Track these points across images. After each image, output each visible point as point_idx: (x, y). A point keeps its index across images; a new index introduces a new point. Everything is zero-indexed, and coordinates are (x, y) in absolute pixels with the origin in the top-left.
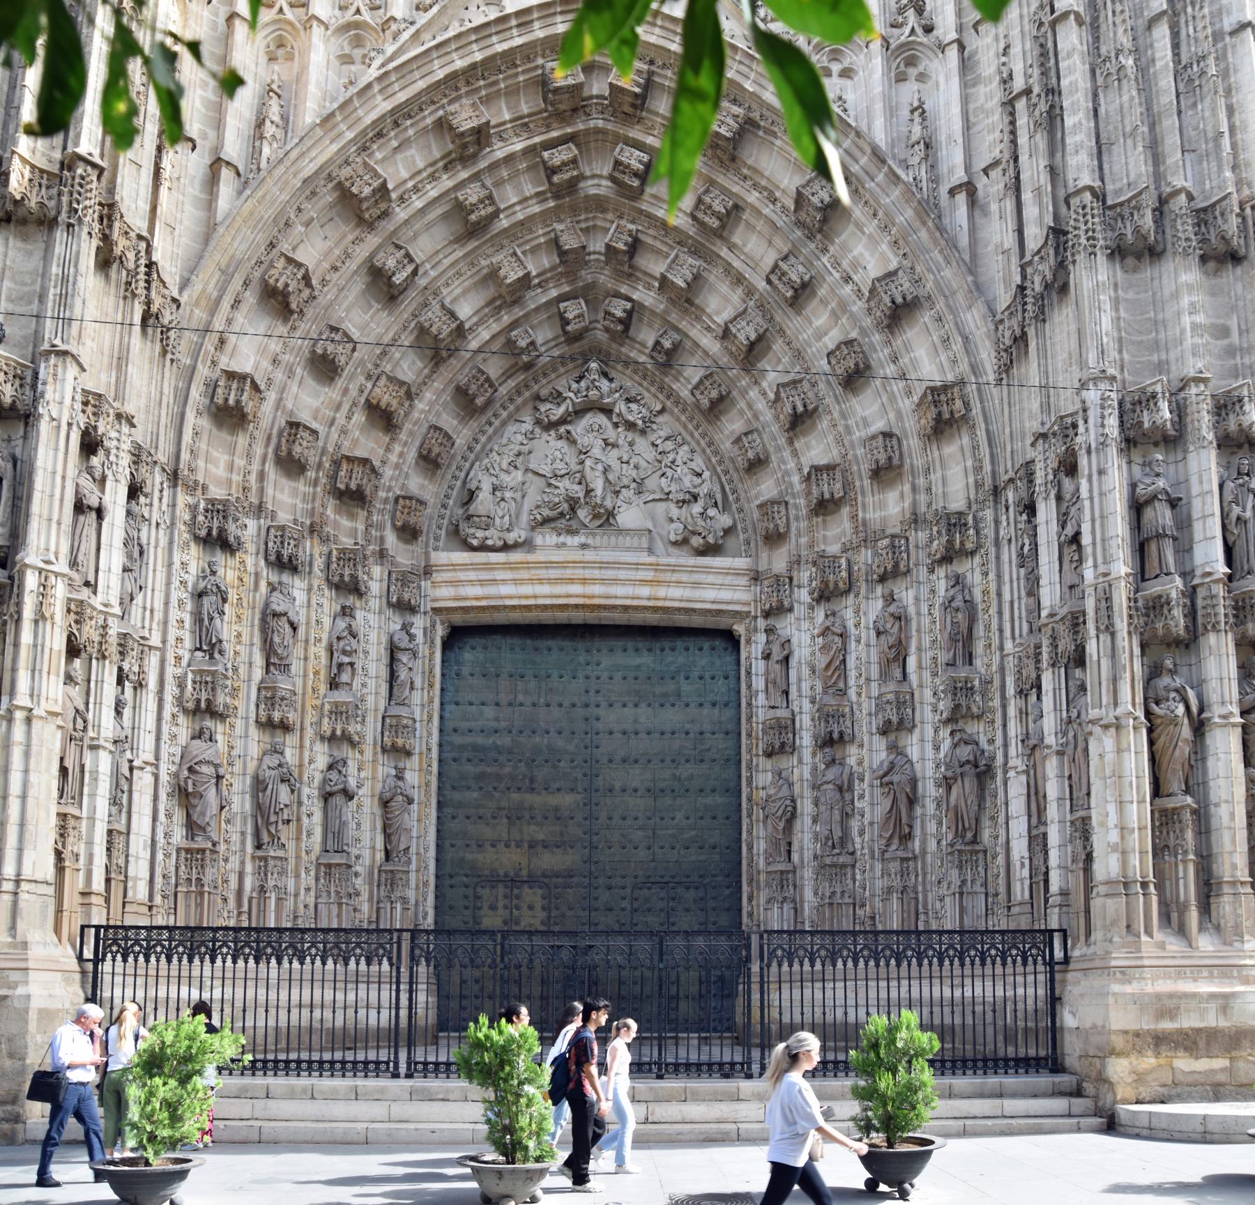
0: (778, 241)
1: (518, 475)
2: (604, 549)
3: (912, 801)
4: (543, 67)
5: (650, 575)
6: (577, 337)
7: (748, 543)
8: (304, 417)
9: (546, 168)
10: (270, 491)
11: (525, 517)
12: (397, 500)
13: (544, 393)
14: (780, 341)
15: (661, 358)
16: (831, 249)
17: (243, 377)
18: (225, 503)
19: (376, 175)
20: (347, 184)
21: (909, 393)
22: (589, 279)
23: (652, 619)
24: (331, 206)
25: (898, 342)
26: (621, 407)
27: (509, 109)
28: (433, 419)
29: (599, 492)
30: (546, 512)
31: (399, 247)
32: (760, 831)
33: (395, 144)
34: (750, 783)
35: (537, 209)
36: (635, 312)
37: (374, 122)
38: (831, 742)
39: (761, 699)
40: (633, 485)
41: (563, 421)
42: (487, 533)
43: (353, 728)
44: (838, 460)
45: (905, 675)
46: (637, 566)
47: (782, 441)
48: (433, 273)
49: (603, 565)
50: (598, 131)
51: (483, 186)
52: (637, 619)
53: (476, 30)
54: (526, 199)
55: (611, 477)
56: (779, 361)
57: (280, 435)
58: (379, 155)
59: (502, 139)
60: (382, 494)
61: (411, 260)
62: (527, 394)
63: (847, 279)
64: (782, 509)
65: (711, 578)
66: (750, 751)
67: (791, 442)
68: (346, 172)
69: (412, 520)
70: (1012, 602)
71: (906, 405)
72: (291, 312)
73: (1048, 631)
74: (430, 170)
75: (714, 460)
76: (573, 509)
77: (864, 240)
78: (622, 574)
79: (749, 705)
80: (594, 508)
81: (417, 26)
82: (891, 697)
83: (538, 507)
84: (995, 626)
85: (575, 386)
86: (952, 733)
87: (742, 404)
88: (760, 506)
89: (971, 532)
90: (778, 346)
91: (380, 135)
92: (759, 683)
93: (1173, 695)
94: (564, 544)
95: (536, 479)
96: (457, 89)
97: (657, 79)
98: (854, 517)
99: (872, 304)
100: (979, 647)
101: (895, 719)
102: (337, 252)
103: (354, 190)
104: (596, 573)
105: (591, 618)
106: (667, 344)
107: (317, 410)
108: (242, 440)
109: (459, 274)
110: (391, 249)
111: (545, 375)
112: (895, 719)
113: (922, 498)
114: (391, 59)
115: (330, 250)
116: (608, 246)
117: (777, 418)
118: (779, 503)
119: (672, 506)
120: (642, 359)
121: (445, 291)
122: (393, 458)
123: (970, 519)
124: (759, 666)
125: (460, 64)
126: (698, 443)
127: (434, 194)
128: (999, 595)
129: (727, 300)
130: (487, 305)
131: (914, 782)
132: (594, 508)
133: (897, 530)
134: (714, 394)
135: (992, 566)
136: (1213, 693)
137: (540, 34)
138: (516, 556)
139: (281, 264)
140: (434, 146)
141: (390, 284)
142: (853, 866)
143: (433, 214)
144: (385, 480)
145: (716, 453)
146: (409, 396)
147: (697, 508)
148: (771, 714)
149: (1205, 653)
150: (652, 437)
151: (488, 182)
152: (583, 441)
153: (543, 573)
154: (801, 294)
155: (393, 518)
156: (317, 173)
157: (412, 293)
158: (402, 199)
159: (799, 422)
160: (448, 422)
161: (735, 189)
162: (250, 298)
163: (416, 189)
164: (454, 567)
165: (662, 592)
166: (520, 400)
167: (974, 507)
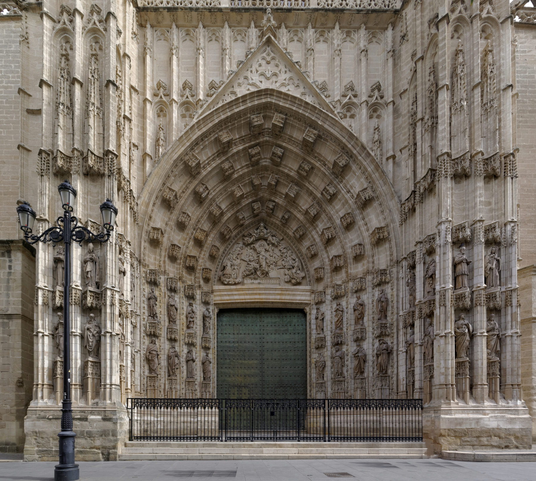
0: (326, 180)
1: (238, 261)
2: (265, 284)
3: (365, 361)
4: (250, 117)
5: (280, 292)
6: (257, 215)
7: (310, 281)
8: (176, 243)
9: (249, 155)
10: (167, 267)
11: (241, 274)
12: (203, 269)
13: (246, 234)
14: (324, 214)
15: (284, 222)
16: (344, 181)
17: (158, 229)
18: (155, 270)
19: (197, 159)
20: (187, 162)
21: (368, 230)
22: (262, 195)
23: (280, 306)
24: (182, 170)
25: (365, 213)
26: (270, 238)
27: (238, 134)
28: (213, 244)
29: (264, 266)
30: (248, 273)
31: (203, 184)
32: (313, 371)
33: (202, 147)
34: (310, 357)
35: (246, 170)
36: (277, 205)
37: (196, 139)
38: (338, 344)
39: (314, 332)
40: (274, 264)
41: (252, 243)
42: (230, 280)
43: (194, 341)
44: (342, 254)
45: (363, 323)
46: (276, 289)
47: (323, 248)
48: (214, 194)
49: (265, 289)
50: (267, 141)
51: (230, 162)
52: (275, 306)
53: (228, 103)
54: (243, 167)
55: (267, 261)
56: (323, 221)
57: (169, 249)
58: (197, 152)
59: (236, 145)
60: (199, 268)
61: (208, 189)
62: (241, 235)
63: (349, 192)
64: (322, 270)
65: (298, 293)
66: (310, 347)
67: (326, 248)
68: (187, 158)
69: (208, 276)
70: (403, 298)
71: (366, 234)
72: (171, 207)
73: (419, 307)
74: (213, 157)
75: (299, 255)
76: (255, 272)
77: (356, 177)
78: (271, 292)
79: (310, 333)
80: (262, 271)
81: (209, 102)
82: (359, 330)
83: (245, 271)
84: (395, 307)
85: (256, 231)
86: (379, 341)
87: (310, 236)
88: (315, 269)
89: (388, 276)
90: (323, 216)
91: (197, 144)
92: (313, 327)
93: (464, 326)
94: (253, 283)
95: (244, 262)
96: (222, 126)
97: (288, 121)
98: (347, 272)
99: (357, 200)
100: (389, 314)
101: (360, 337)
102: (184, 186)
103: (190, 164)
104: (263, 292)
105: (262, 306)
106: (286, 217)
107: (179, 241)
108: (158, 251)
109: (221, 194)
110: (201, 185)
111: (246, 228)
112: (360, 337)
113: (371, 265)
114: (201, 115)
115: (182, 186)
116: (269, 183)
117: (321, 240)
118: (321, 268)
119: (286, 270)
120: (277, 222)
121: (217, 200)
122: (202, 256)
123: (388, 272)
124: (313, 321)
125: (223, 117)
126: (294, 250)
127: (214, 165)
128: (398, 296)
129: (307, 201)
130: (230, 204)
131: (365, 355)
132: (262, 271)
133: (361, 276)
134: (301, 233)
135: (395, 287)
136: (478, 325)
137: (250, 105)
138: (239, 287)
139: (167, 190)
140: (214, 148)
141: (201, 197)
142: (344, 381)
143: (213, 173)
144: (200, 263)
145: (300, 253)
146: (207, 236)
147: (294, 271)
148: (318, 336)
149: (475, 312)
150: (280, 248)
151: (231, 161)
152: (259, 249)
153: (247, 292)
154: (333, 197)
155: (202, 275)
156: (178, 158)
157: (207, 201)
158: (204, 167)
159: (329, 242)
160: (218, 244)
161: (312, 161)
162: (158, 202)
163: (208, 164)
164: (220, 290)
165: (283, 297)
166: (239, 237)
167: (389, 268)
